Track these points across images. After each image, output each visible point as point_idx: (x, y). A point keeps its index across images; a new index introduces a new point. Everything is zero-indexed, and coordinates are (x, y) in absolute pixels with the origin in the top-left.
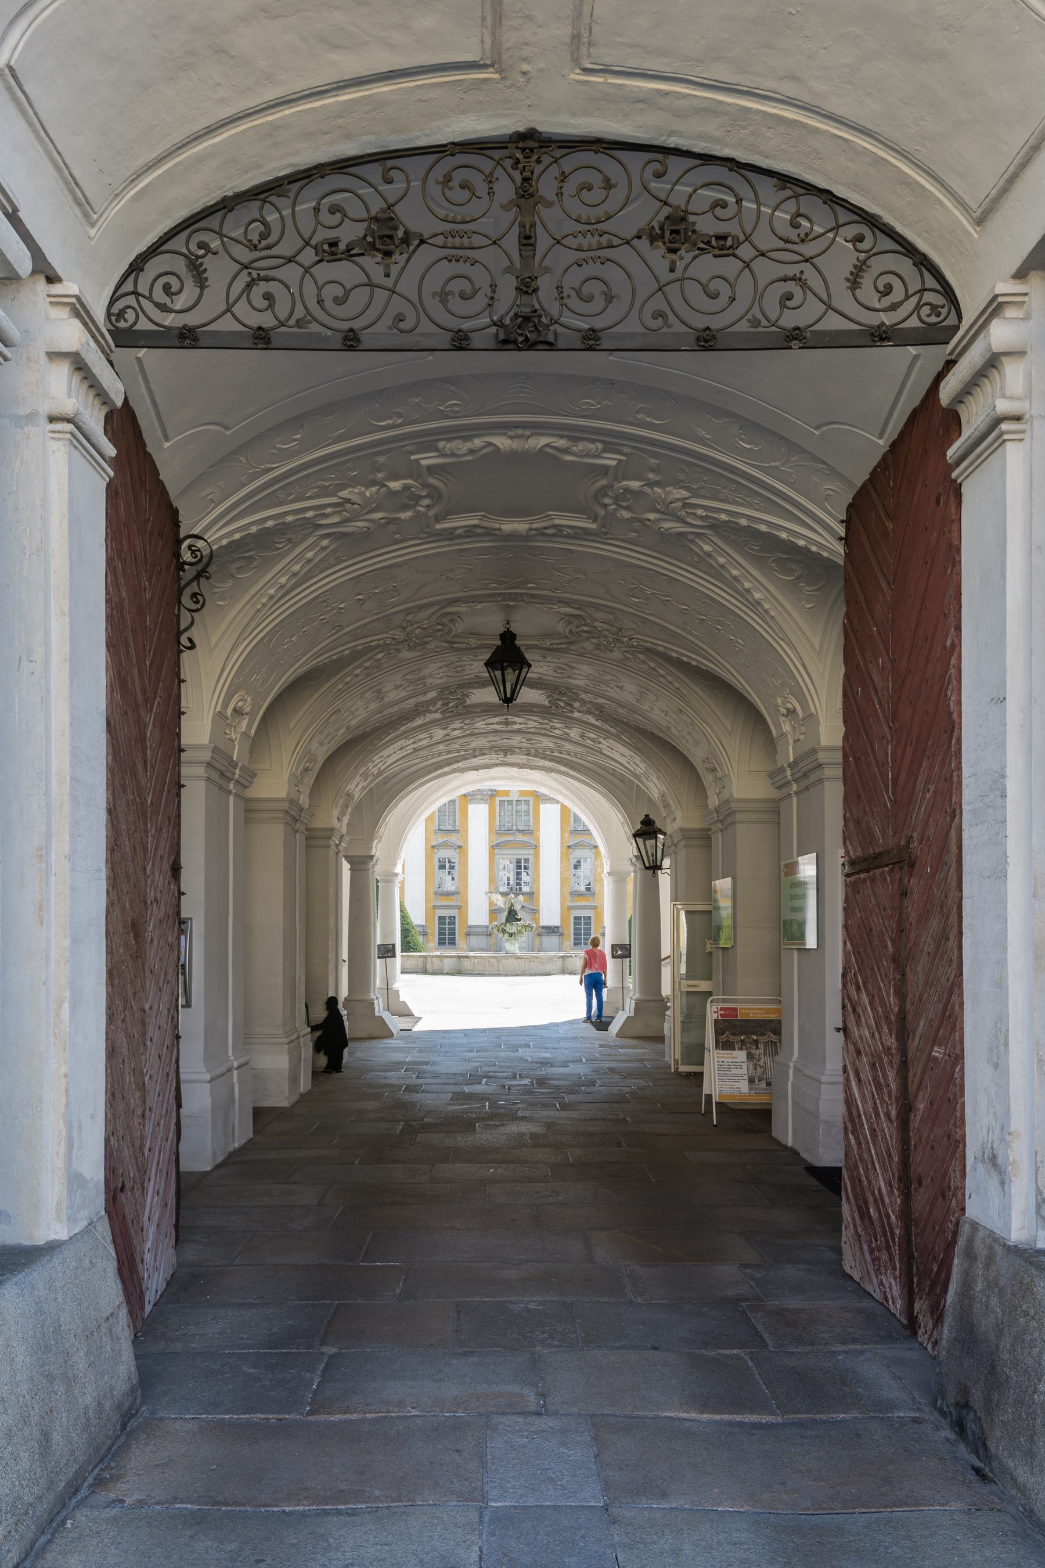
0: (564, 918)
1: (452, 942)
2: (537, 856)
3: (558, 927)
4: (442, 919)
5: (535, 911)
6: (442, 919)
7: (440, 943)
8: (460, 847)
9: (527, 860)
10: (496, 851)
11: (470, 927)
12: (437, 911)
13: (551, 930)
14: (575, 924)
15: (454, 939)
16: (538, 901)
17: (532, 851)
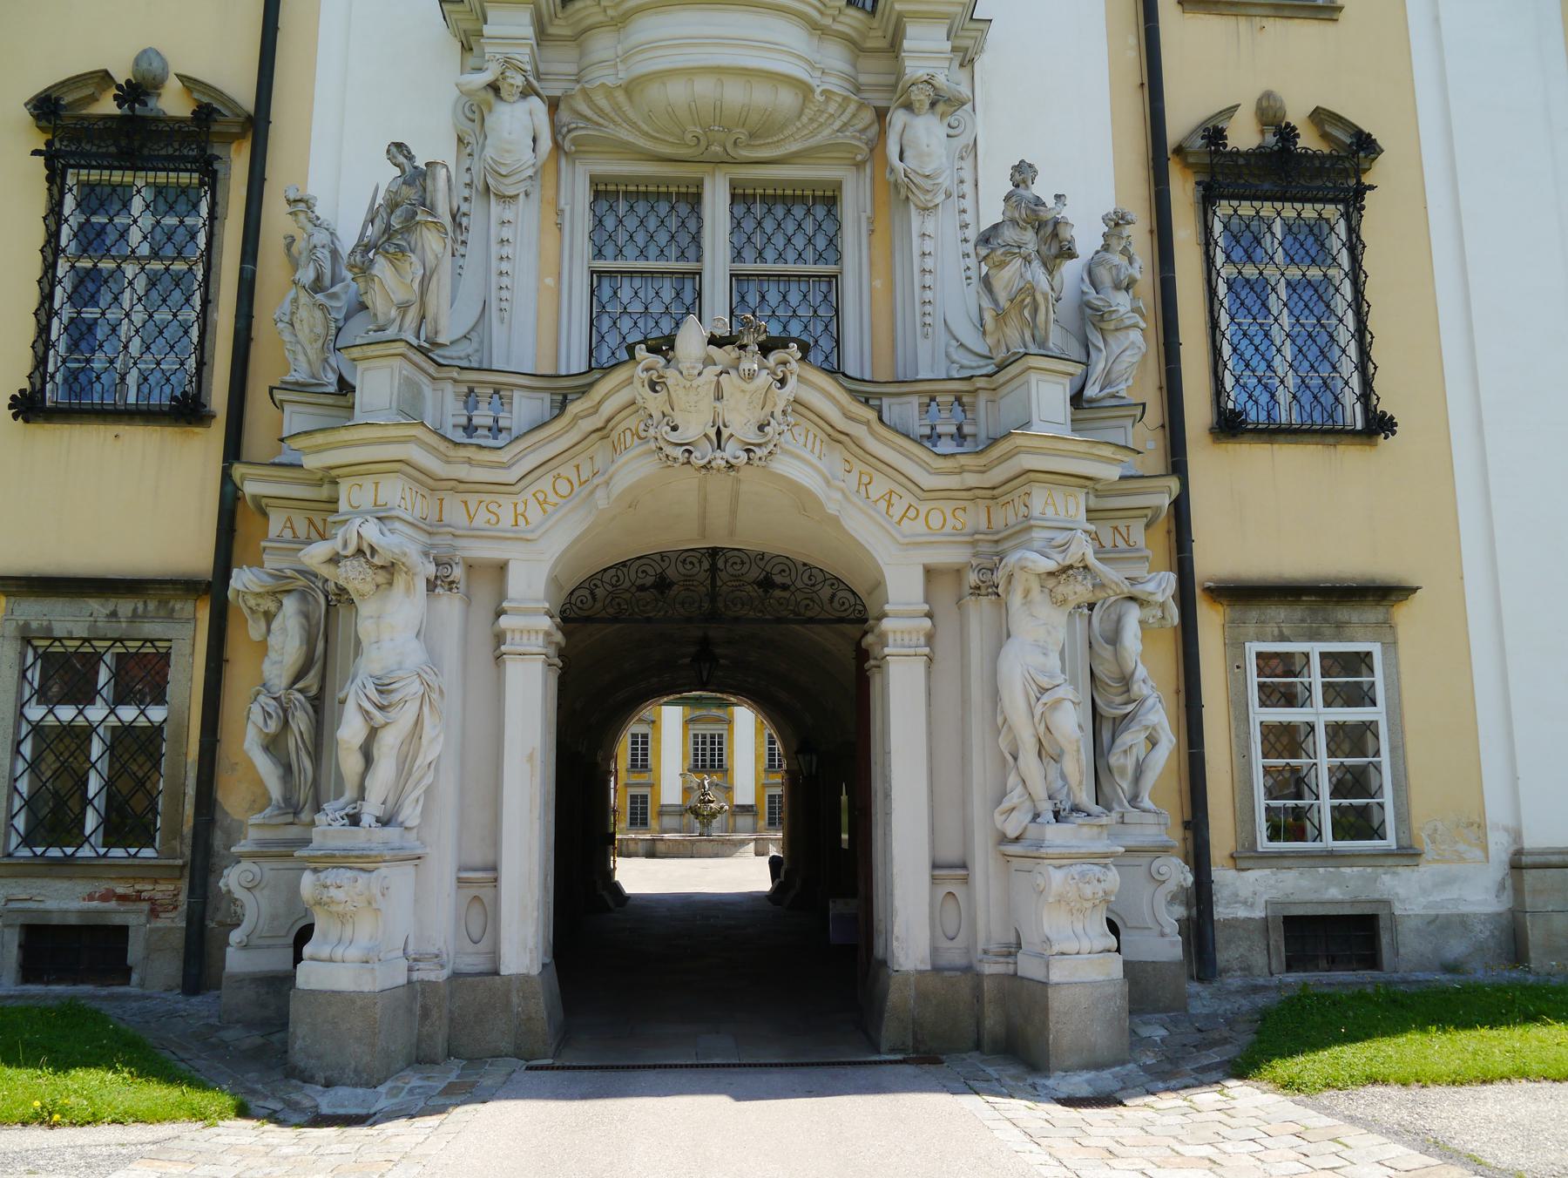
0: (758, 796)
1: (644, 823)
2: (731, 731)
3: (752, 806)
4: (634, 798)
5: (729, 789)
6: (634, 798)
7: (631, 824)
8: (653, 722)
9: (721, 736)
10: (690, 726)
11: (663, 806)
12: (629, 789)
13: (745, 809)
14: (770, 802)
15: (646, 819)
16: (732, 778)
17: (726, 727)
